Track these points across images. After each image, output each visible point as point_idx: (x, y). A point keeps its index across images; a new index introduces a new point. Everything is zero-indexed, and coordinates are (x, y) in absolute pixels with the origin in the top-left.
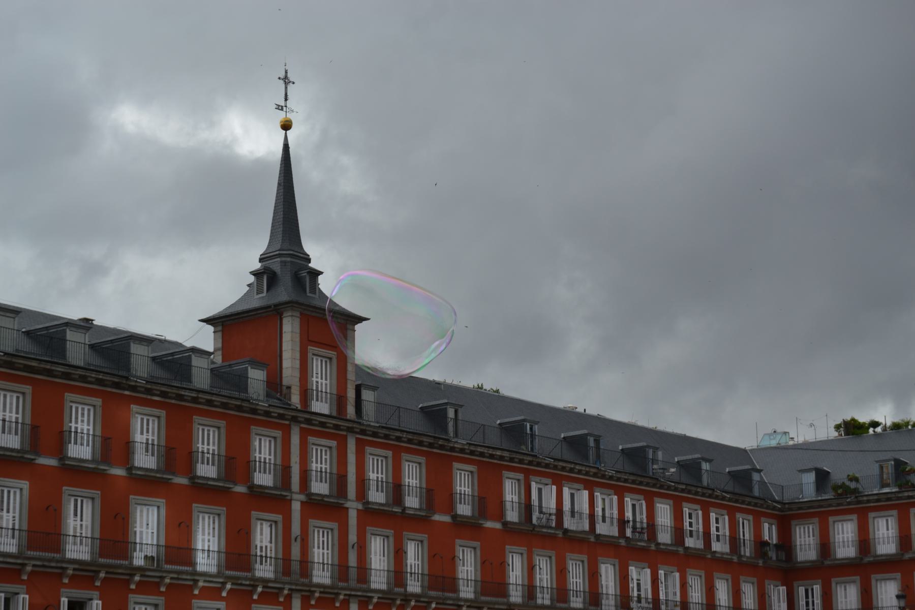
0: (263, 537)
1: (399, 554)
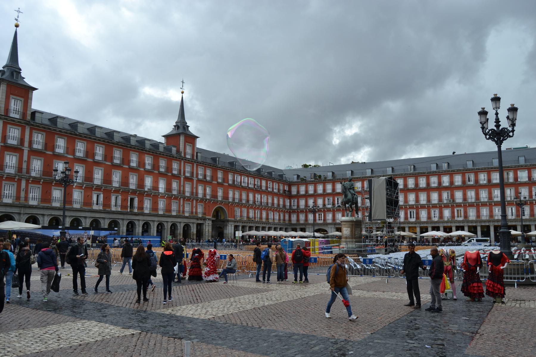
0: (175, 185)
1: (205, 190)
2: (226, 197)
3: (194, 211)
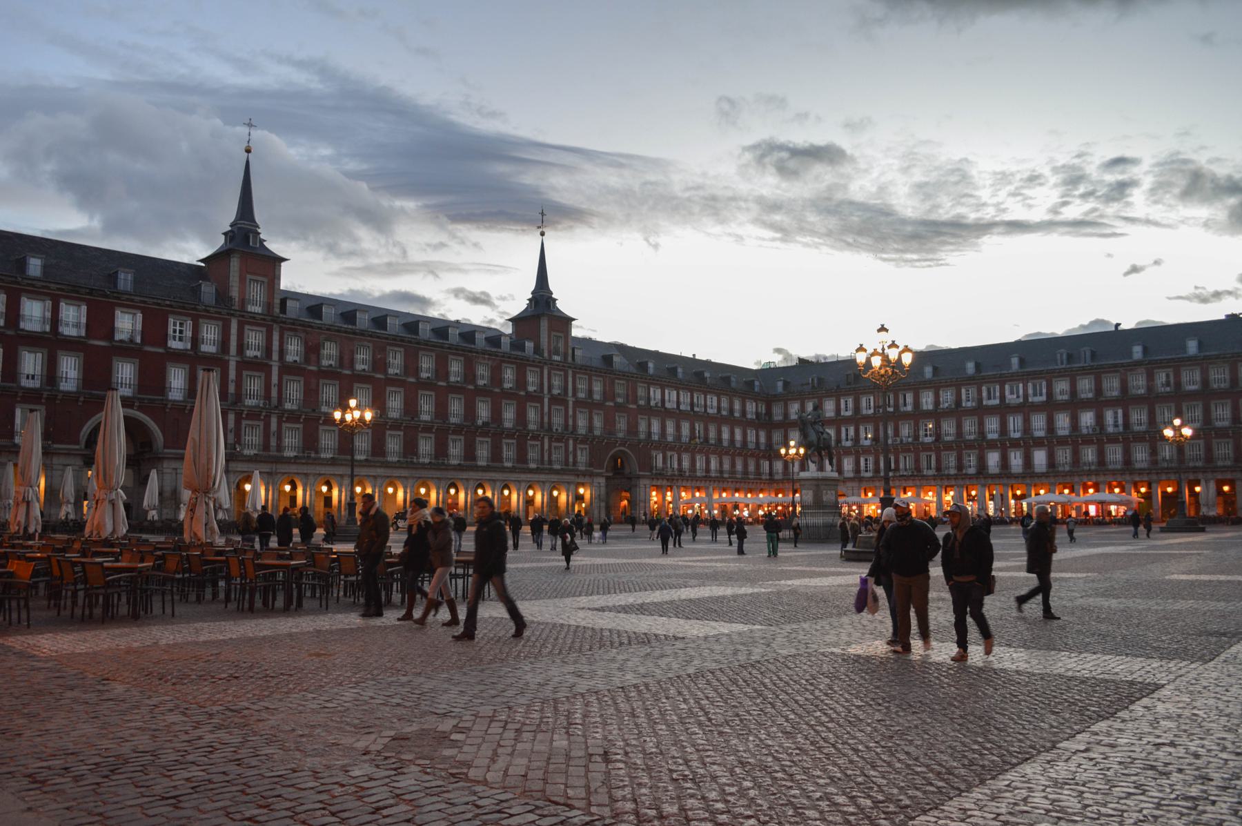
0: (532, 415)
3: (571, 460)
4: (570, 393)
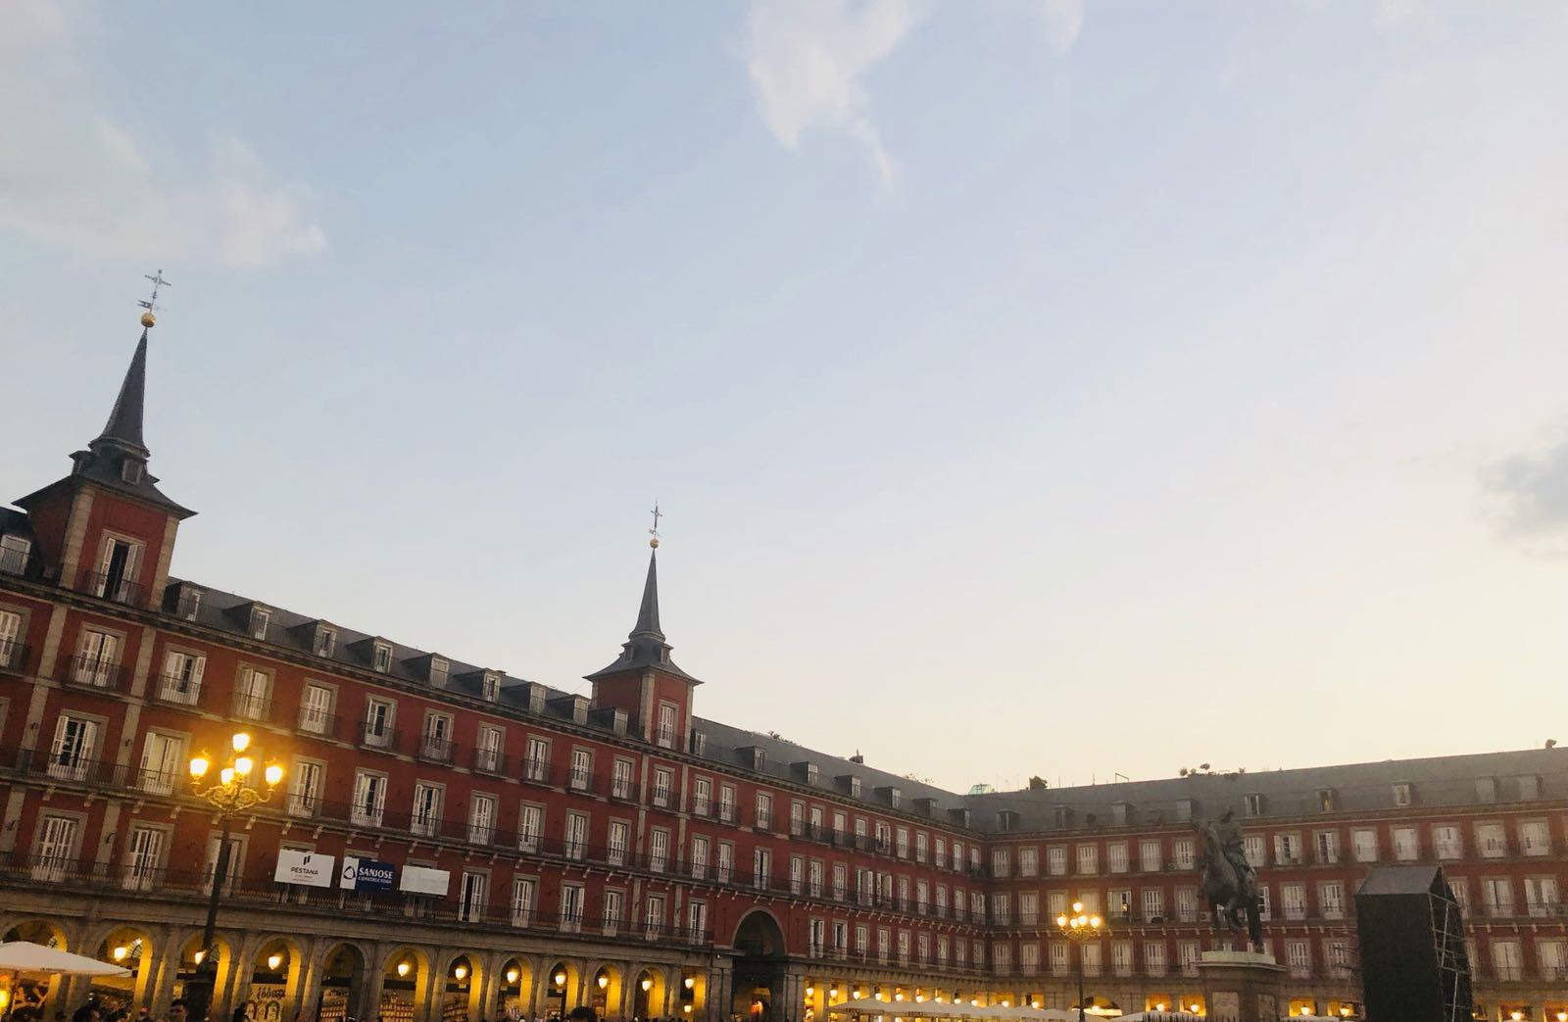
0: (617, 837)
1: (714, 853)
2: (781, 880)
4: (683, 807)
